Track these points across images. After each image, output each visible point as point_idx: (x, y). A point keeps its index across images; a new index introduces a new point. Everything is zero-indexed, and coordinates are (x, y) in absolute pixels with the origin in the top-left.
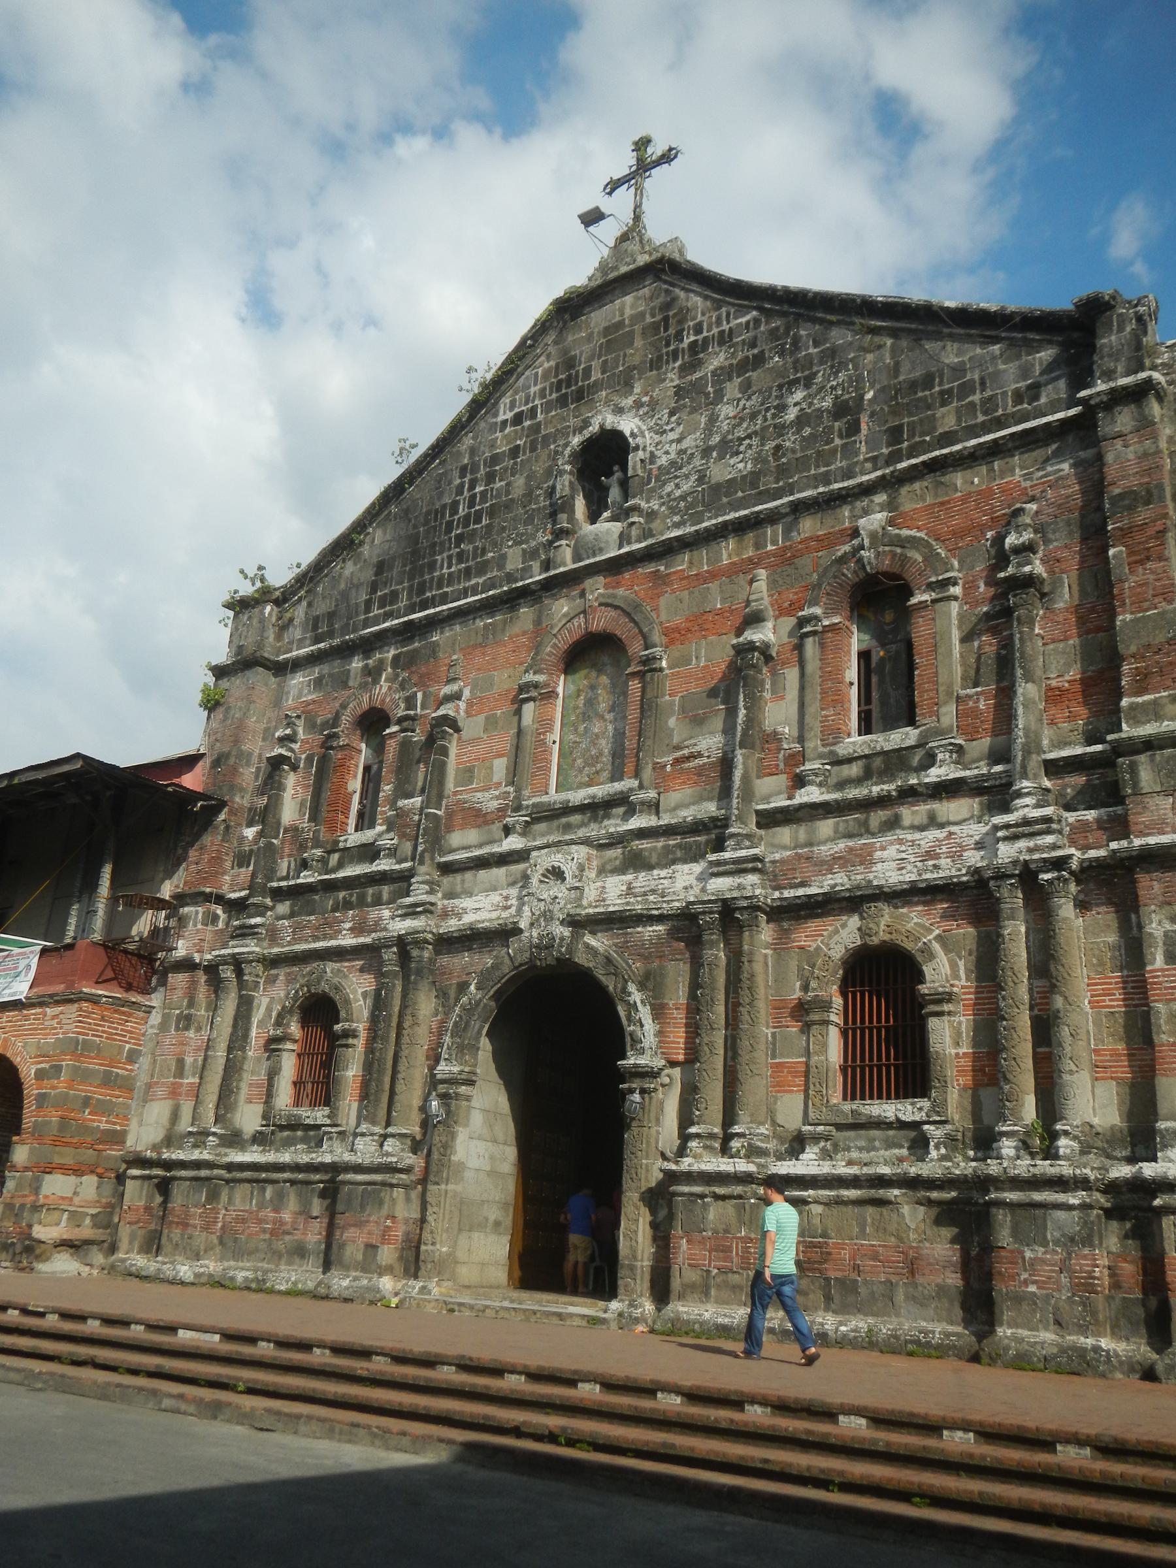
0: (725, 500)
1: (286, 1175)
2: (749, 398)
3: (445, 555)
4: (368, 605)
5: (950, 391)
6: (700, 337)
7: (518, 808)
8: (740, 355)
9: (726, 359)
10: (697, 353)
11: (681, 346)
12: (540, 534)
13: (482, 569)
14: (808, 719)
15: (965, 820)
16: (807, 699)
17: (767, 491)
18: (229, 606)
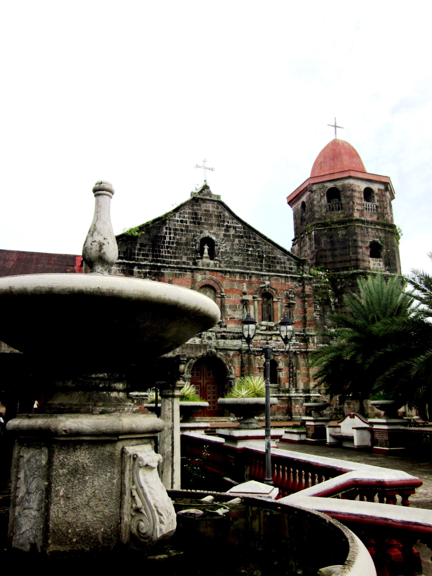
0: (237, 265)
2: (240, 244)
3: (163, 250)
12: (191, 255)
13: (175, 258)
16: (256, 313)
17: (245, 267)
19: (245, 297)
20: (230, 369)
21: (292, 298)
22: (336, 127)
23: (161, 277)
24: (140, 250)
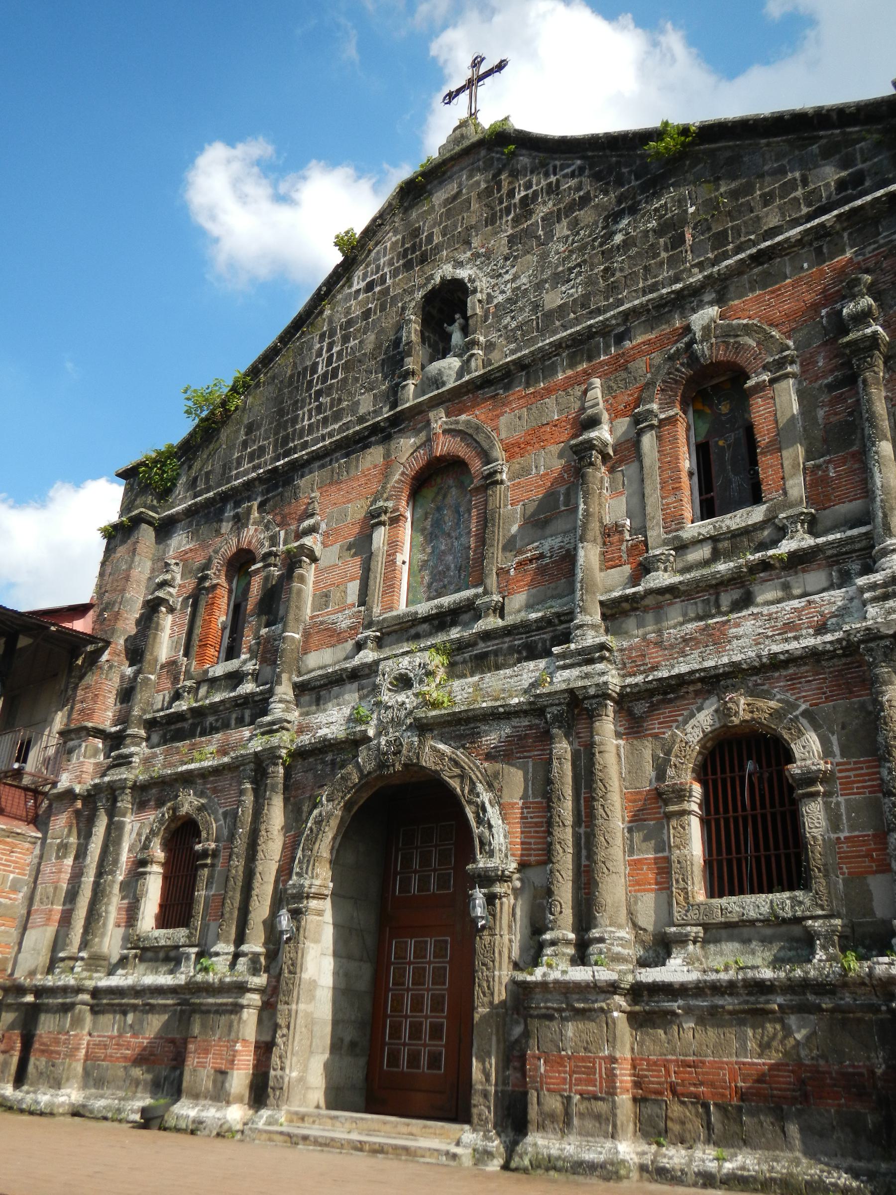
0: (558, 323)
3: (306, 409)
5: (771, 194)
6: (532, 190)
7: (369, 626)
8: (567, 200)
9: (554, 205)
10: (528, 205)
11: (513, 202)
13: (337, 417)
14: (649, 509)
15: (824, 590)
16: (648, 491)
18: (119, 475)
20: (480, 821)
21: (862, 318)
23: (290, 503)
24: (245, 444)
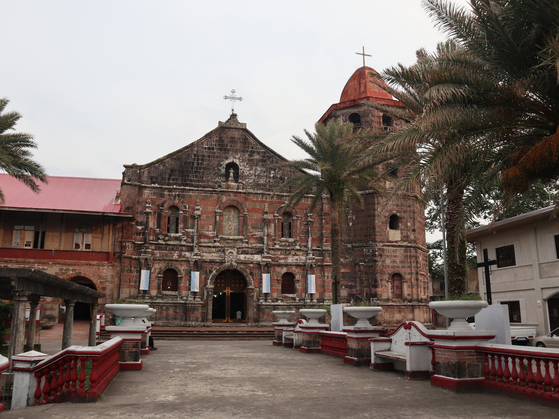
1: (169, 305)
4: (169, 179)
7: (218, 237)
12: (217, 179)
13: (203, 181)
19: (265, 216)
22: (364, 55)
